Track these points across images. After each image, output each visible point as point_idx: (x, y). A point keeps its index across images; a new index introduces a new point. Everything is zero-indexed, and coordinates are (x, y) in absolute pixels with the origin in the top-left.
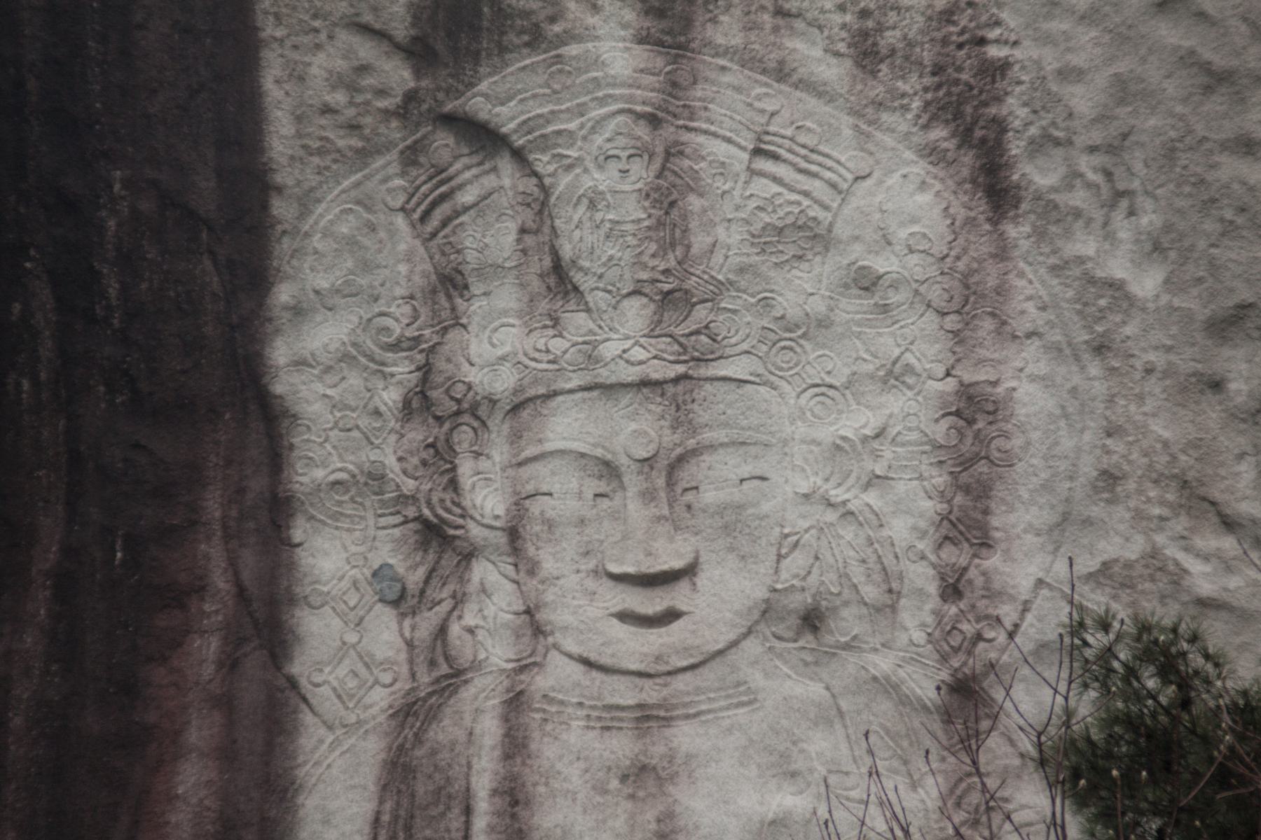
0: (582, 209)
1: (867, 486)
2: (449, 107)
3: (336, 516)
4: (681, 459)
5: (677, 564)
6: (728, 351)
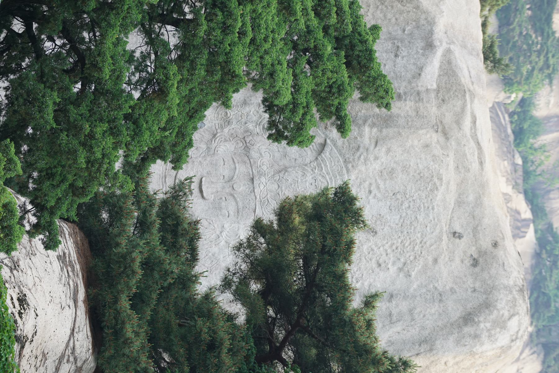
0: (301, 173)
1: (226, 242)
2: (328, 141)
3: (218, 113)
4: (234, 197)
5: (205, 195)
6: (263, 209)
